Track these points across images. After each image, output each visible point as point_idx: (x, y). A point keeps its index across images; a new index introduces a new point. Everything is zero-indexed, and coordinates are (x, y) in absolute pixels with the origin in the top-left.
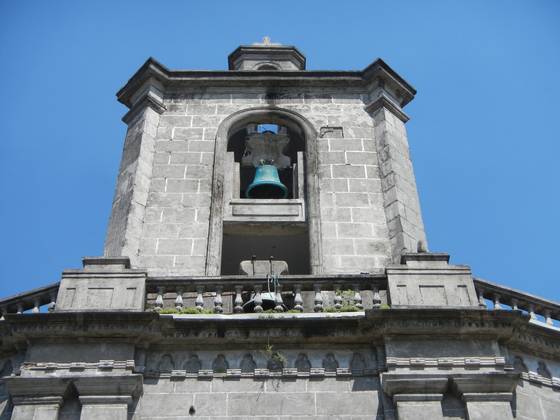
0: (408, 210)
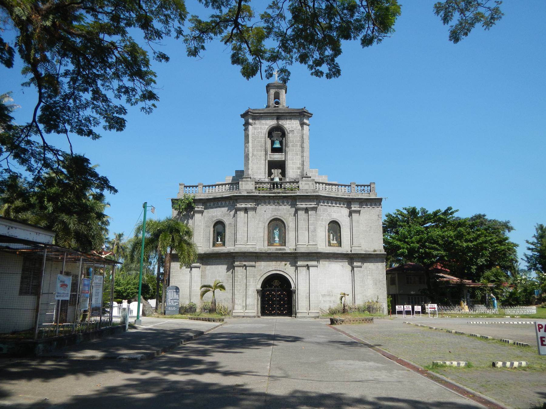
0: (306, 158)
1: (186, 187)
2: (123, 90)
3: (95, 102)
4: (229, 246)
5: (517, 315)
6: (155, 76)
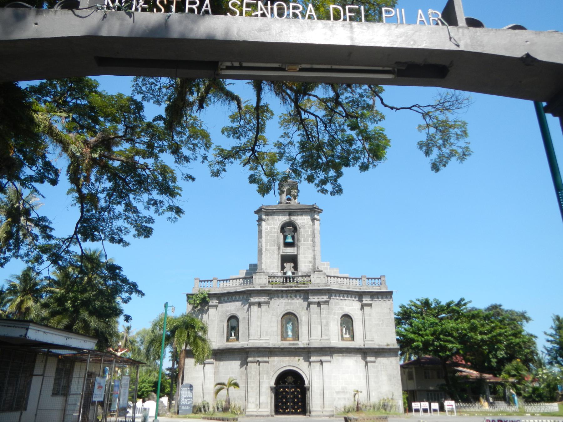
1: (201, 281)
2: (152, 202)
3: (127, 214)
4: (243, 341)
5: (538, 413)
6: (181, 190)
